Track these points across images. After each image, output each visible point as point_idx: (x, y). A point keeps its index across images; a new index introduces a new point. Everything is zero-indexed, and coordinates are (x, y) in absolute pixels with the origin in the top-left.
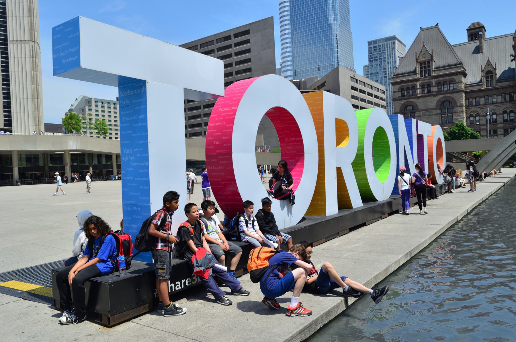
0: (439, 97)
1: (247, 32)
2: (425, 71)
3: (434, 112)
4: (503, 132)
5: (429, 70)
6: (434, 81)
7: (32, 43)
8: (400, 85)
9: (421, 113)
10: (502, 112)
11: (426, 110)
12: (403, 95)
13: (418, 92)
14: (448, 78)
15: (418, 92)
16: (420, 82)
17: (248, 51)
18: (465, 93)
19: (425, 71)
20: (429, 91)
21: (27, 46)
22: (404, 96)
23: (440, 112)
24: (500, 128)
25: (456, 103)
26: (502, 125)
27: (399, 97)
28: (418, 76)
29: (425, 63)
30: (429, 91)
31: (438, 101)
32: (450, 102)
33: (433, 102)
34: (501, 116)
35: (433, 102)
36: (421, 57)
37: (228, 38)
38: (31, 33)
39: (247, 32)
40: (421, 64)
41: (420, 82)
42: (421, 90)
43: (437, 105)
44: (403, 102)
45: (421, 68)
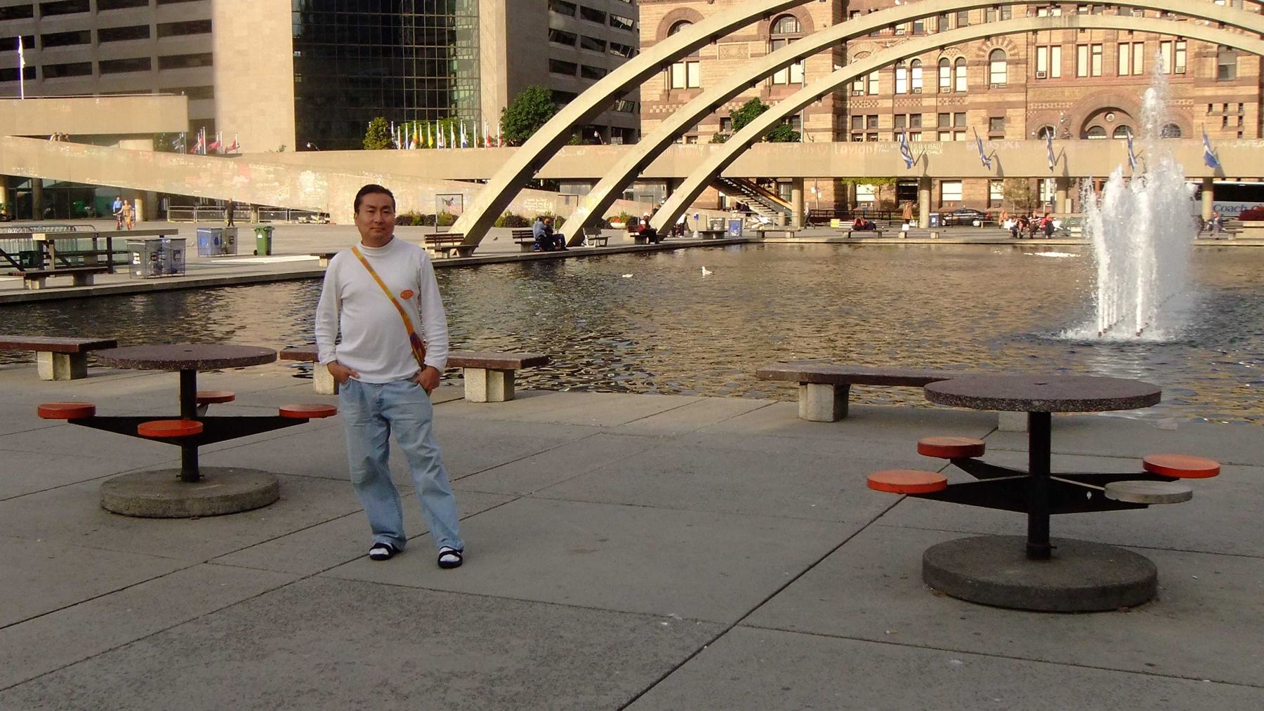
4: (934, 123)
10: (935, 63)
24: (928, 110)
26: (932, 102)
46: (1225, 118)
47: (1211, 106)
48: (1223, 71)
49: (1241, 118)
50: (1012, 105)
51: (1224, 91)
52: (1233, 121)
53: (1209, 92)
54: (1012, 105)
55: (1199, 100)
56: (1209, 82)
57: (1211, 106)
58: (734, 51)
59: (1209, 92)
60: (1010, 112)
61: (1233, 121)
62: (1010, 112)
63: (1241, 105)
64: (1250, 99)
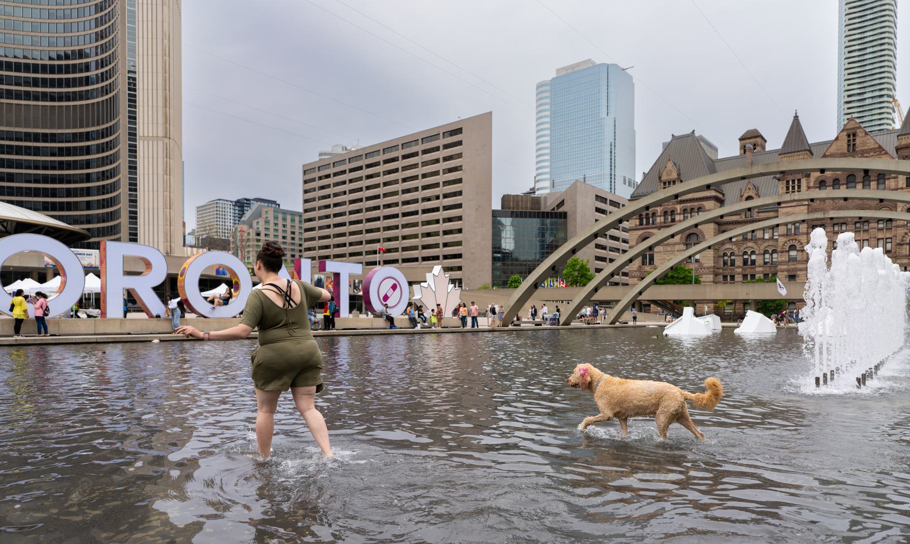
1: (459, 131)
3: (677, 247)
6: (679, 207)
7: (166, 140)
12: (641, 224)
13: (660, 220)
14: (696, 204)
17: (459, 156)
21: (160, 143)
25: (704, 237)
34: (761, 257)
36: (664, 174)
37: (435, 137)
38: (166, 128)
39: (459, 131)
42: (662, 218)
44: (640, 232)
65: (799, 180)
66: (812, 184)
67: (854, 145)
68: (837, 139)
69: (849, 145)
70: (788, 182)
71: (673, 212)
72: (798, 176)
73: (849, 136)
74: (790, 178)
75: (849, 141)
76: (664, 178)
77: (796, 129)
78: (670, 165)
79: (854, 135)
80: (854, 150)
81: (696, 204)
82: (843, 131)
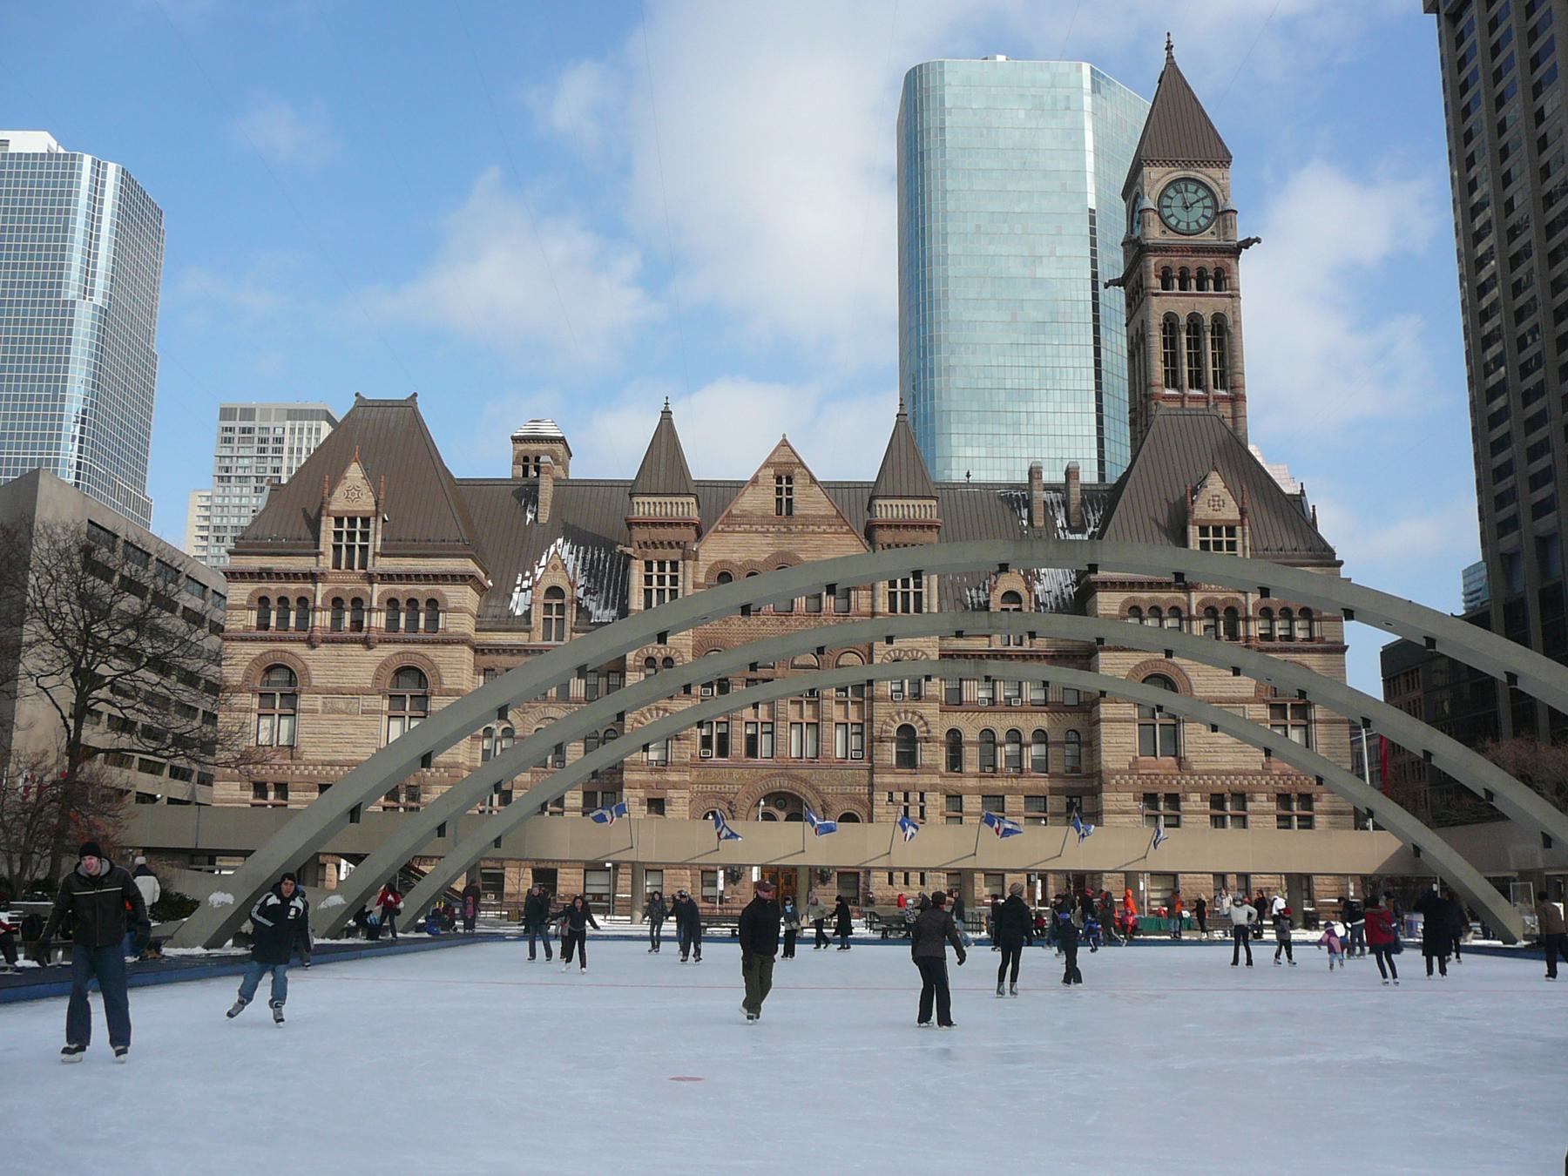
0: (384, 652)
2: (350, 549)
4: (580, 803)
5: (364, 549)
8: (255, 586)
9: (319, 702)
11: (339, 691)
12: (263, 625)
13: (322, 619)
15: (322, 619)
16: (328, 587)
18: (479, 650)
19: (350, 549)
20: (357, 625)
22: (267, 627)
23: (386, 704)
27: (247, 629)
28: (327, 562)
29: (352, 521)
30: (357, 625)
31: (384, 665)
32: (422, 674)
33: (361, 666)
35: (361, 666)
36: (339, 493)
40: (339, 521)
41: (328, 587)
43: (377, 678)
44: (257, 649)
45: (338, 535)
46: (906, 808)
47: (891, 794)
48: (908, 759)
49: (922, 808)
50: (675, 786)
51: (905, 779)
52: (914, 812)
53: (888, 779)
54: (675, 786)
55: (884, 787)
56: (888, 769)
57: (891, 794)
58: (341, 705)
59: (888, 779)
60: (671, 793)
61: (914, 812)
62: (671, 793)
63: (922, 795)
64: (933, 788)
65: (674, 565)
66: (701, 579)
67: (789, 501)
68: (755, 481)
69: (779, 501)
70: (649, 566)
71: (357, 603)
72: (675, 554)
73: (779, 480)
74: (655, 554)
75: (779, 491)
76: (339, 502)
77: (665, 445)
78: (355, 472)
79: (789, 480)
80: (790, 513)
81: (422, 590)
82: (767, 465)
